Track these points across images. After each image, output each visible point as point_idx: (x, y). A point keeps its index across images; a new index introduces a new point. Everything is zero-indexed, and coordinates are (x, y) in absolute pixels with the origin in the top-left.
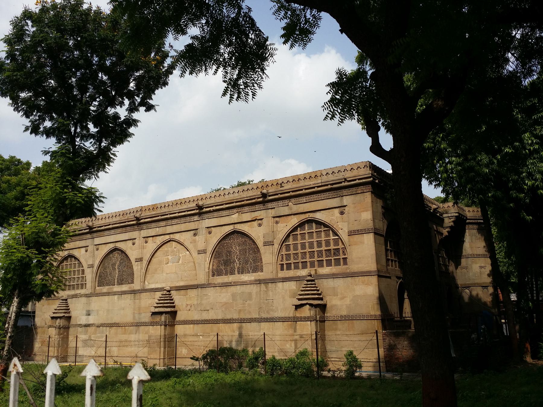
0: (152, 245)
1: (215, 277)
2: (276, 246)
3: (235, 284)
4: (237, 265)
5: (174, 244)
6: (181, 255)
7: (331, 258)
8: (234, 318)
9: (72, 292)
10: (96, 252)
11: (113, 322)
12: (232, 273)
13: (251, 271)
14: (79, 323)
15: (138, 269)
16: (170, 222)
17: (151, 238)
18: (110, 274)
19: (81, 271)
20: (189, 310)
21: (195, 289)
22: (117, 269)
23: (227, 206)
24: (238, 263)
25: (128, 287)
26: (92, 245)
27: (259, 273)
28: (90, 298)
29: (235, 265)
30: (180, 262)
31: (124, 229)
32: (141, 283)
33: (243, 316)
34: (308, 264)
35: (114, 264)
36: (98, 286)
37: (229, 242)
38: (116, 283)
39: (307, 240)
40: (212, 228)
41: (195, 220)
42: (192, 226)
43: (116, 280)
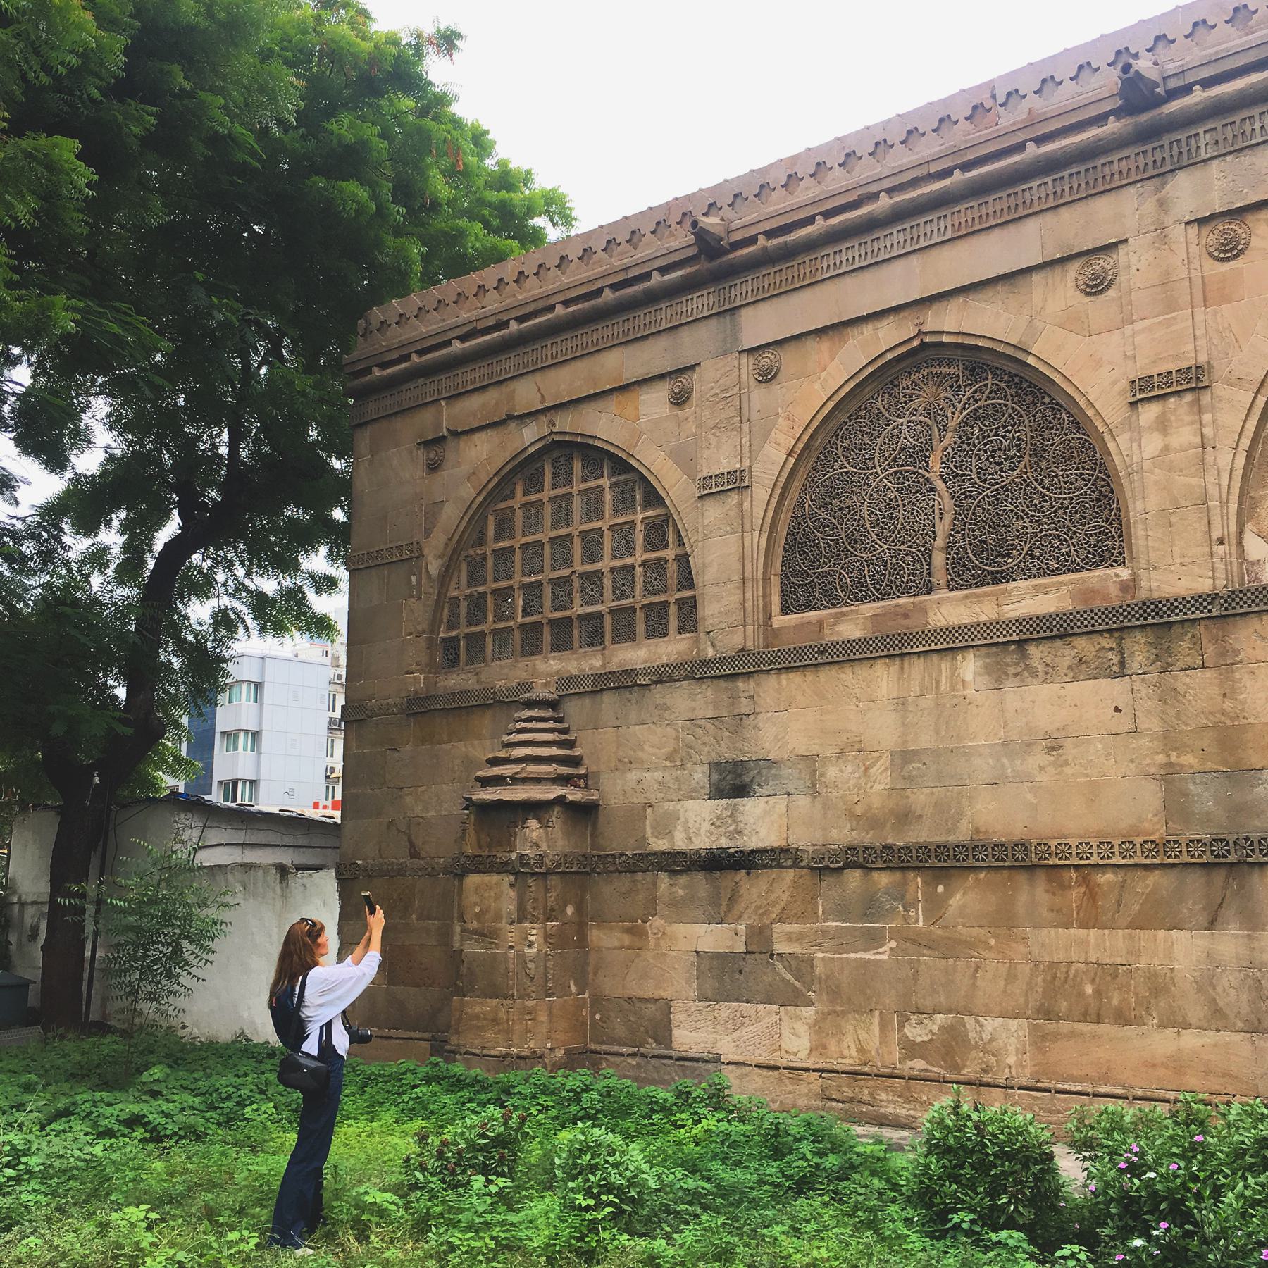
9: (588, 662)
10: (759, 397)
11: (963, 834)
14: (660, 845)
15: (1166, 449)
18: (885, 525)
19: (640, 526)
22: (940, 485)
25: (1064, 590)
26: (725, 353)
28: (740, 684)
31: (996, 203)
32: (1220, 550)
35: (917, 455)
36: (785, 610)
38: (939, 577)
43: (939, 559)
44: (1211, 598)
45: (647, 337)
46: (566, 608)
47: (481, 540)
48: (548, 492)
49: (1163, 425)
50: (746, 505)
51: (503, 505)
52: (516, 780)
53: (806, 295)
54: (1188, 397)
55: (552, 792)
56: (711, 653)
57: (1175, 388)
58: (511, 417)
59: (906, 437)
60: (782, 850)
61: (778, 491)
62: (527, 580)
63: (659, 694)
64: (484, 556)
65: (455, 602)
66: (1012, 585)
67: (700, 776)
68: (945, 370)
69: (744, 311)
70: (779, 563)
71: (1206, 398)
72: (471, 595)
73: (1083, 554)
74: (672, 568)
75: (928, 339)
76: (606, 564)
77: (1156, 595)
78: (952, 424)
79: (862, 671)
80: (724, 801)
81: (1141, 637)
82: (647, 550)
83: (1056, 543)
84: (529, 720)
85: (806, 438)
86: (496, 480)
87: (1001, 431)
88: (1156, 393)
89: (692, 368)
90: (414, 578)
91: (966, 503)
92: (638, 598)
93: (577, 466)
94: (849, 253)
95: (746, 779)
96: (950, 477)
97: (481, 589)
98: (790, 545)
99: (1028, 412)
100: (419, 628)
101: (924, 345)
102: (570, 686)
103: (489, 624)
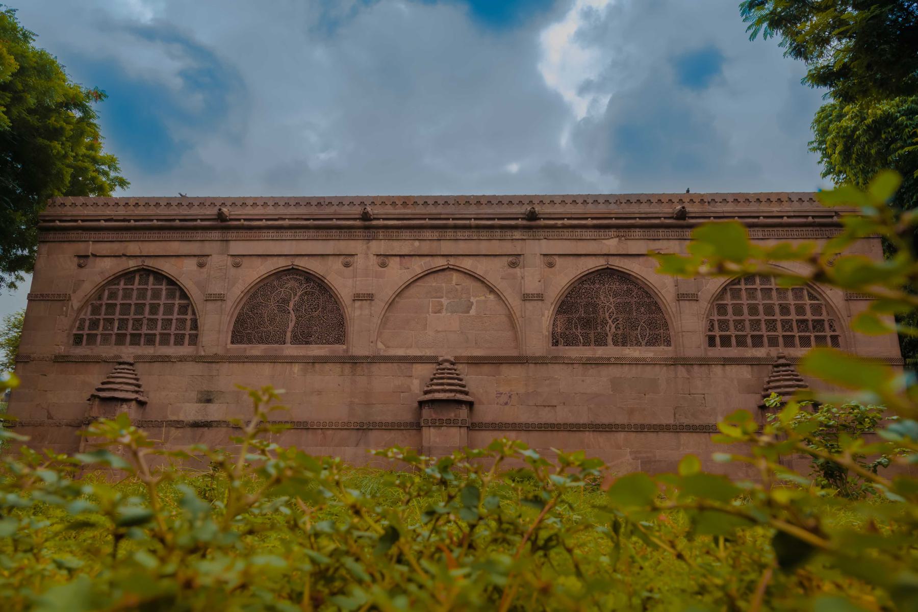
0: (397, 273)
1: (560, 347)
2: (704, 304)
3: (620, 362)
4: (611, 328)
5: (454, 278)
6: (472, 299)
7: (807, 334)
8: (617, 422)
9: (149, 351)
12: (601, 341)
13: (643, 343)
14: (175, 418)
16: (450, 234)
17: (398, 259)
19: (177, 306)
20: (506, 404)
21: (519, 366)
23: (595, 222)
24: (613, 326)
25: (327, 349)
26: (222, 254)
27: (662, 347)
28: (214, 365)
29: (608, 329)
30: (473, 312)
31: (322, 233)
32: (371, 344)
33: (637, 419)
34: (765, 340)
35: (286, 301)
36: (232, 343)
37: (592, 287)
38: (288, 339)
39: (745, 301)
40: (557, 258)
41: (514, 237)
42: (507, 247)
43: (289, 335)
44: (368, 357)
45: (191, 241)
46: (138, 330)
47: (100, 298)
48: (136, 285)
49: (361, 308)
50: (224, 306)
51: (114, 287)
52: (115, 390)
53: (256, 243)
54: (369, 302)
55: (134, 396)
56: (203, 354)
57: (366, 298)
58: (124, 255)
59: (283, 295)
60: (223, 421)
61: (236, 304)
62: (122, 317)
63: (179, 365)
64: (101, 305)
65: (83, 320)
66: (311, 345)
67: (194, 395)
68: (298, 277)
69: (231, 242)
70: (232, 327)
71: (373, 303)
72: (92, 319)
73: (333, 340)
74: (189, 323)
75: (294, 267)
76: (160, 316)
77: (353, 355)
78: (299, 294)
79: (260, 366)
80: (202, 404)
81: (348, 365)
82: (178, 314)
83: (326, 335)
84: (124, 369)
85: (248, 288)
86: (113, 277)
87: (313, 300)
88: (361, 298)
89: (208, 256)
90: (65, 308)
91: (300, 319)
92: (173, 330)
93: (151, 279)
94: (272, 234)
95: (212, 397)
96: (296, 310)
97: (97, 317)
98: (237, 322)
99: (322, 295)
100: (65, 328)
101: (293, 268)
102: (139, 359)
103: (100, 330)
